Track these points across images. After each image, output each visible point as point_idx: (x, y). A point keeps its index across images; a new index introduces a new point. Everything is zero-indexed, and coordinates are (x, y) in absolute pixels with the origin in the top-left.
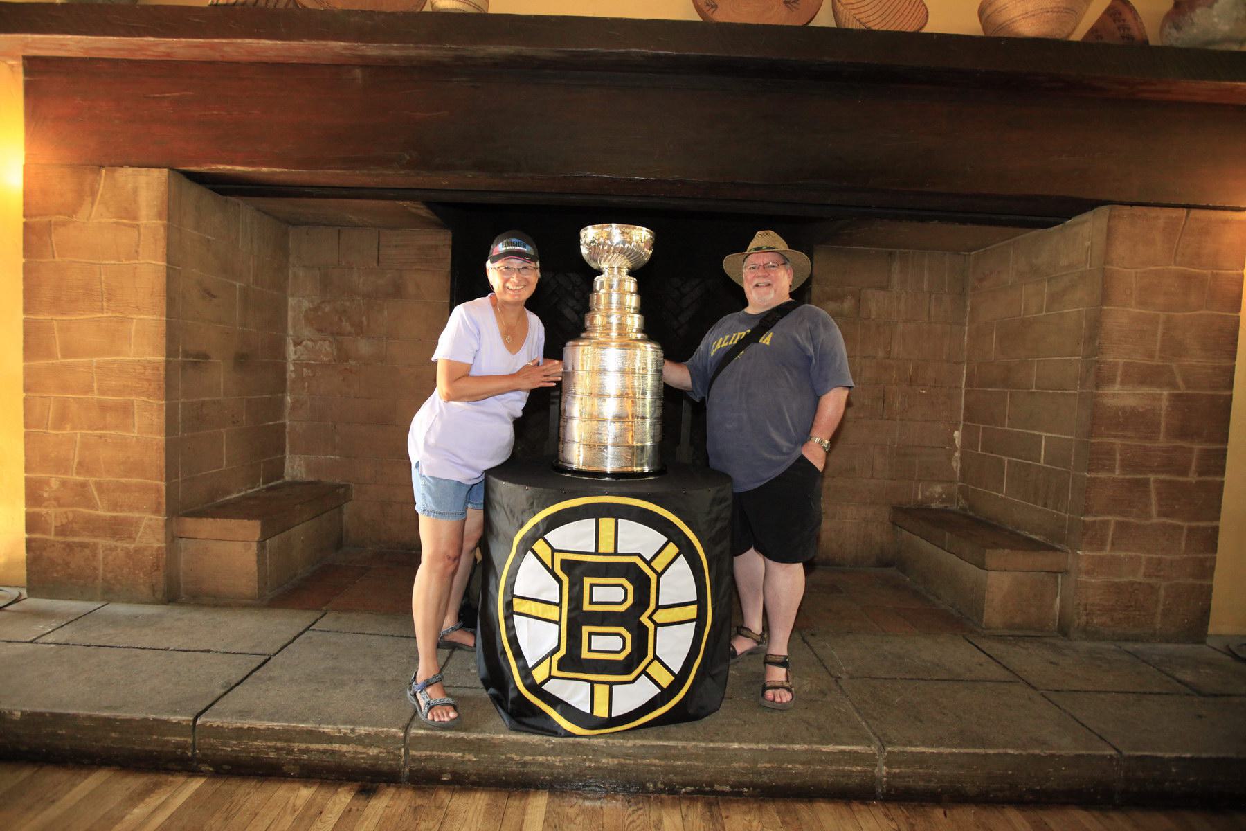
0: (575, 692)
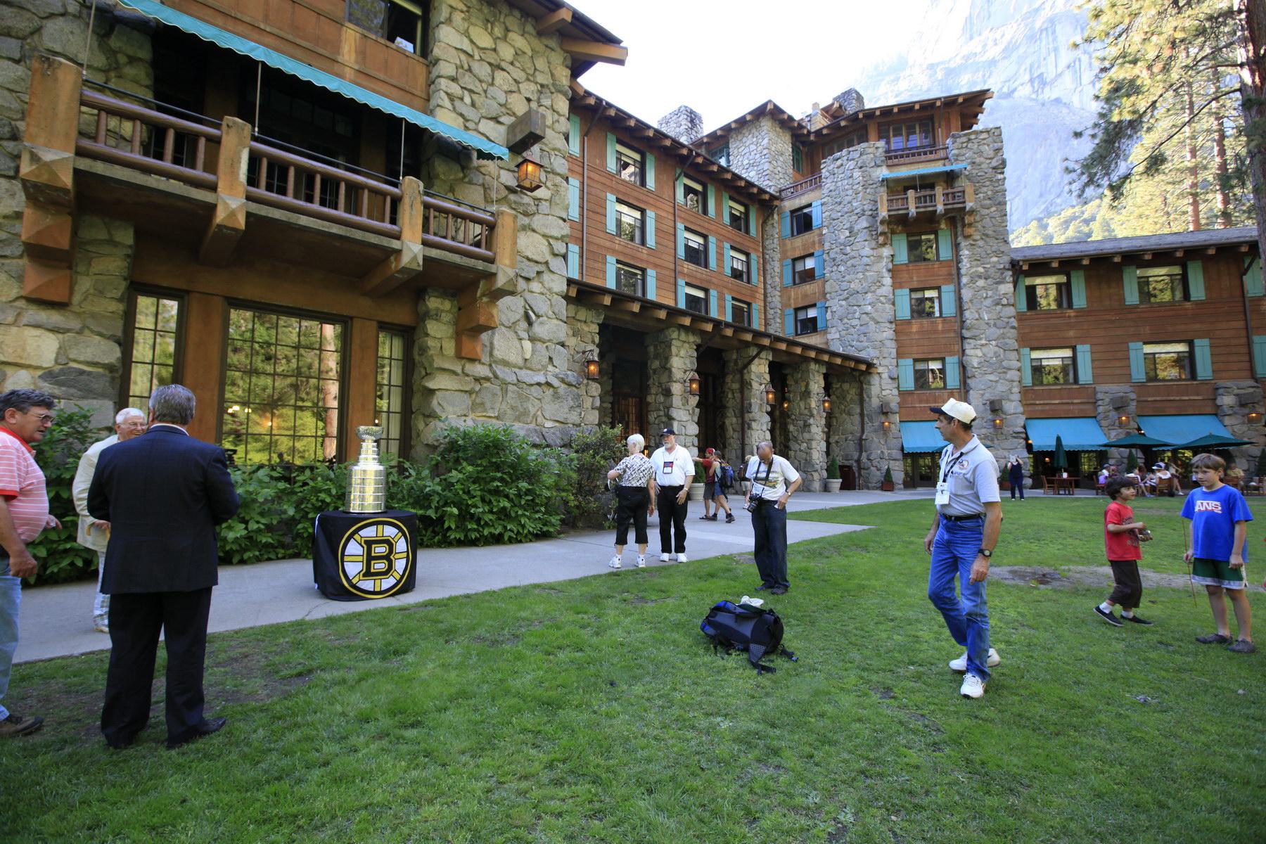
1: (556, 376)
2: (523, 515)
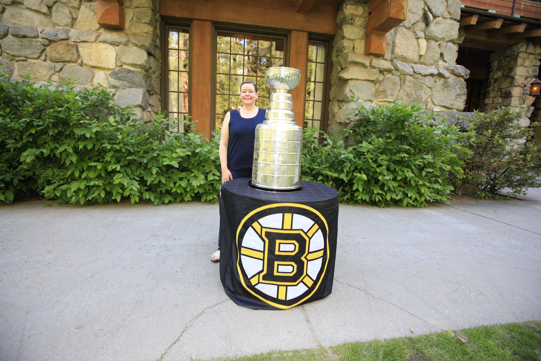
0: (269, 289)
1: (447, 69)
2: (424, 185)
